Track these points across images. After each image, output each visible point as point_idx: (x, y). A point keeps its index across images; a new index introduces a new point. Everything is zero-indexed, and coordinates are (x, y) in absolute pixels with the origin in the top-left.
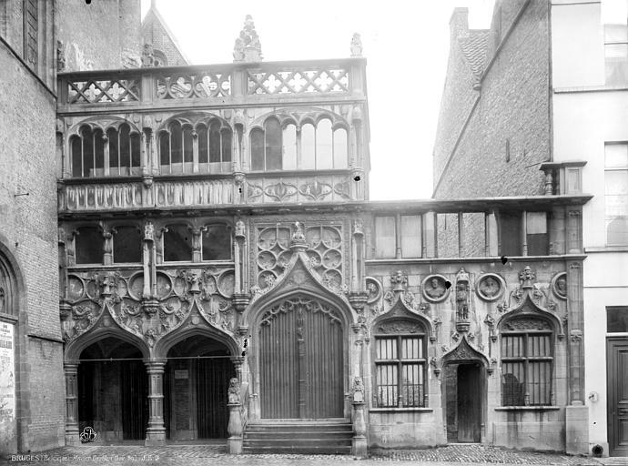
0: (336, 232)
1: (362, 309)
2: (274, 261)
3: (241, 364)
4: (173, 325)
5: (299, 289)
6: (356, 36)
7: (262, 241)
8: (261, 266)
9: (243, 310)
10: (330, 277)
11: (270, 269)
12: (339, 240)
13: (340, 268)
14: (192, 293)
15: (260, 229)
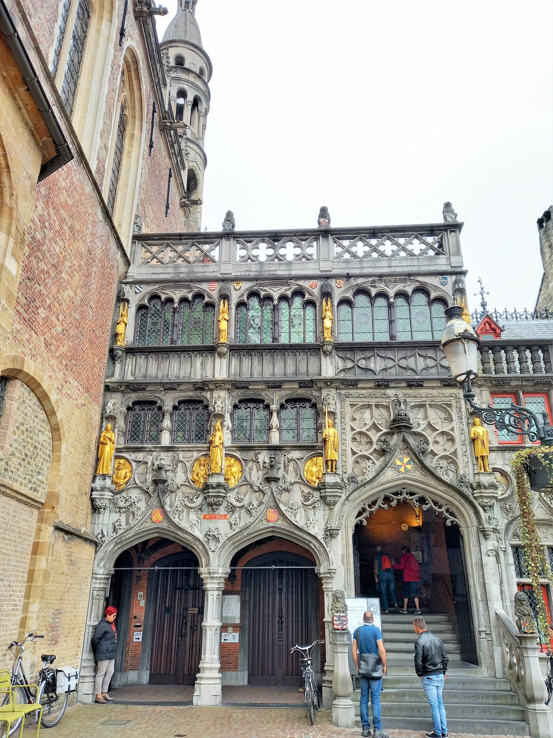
0: (446, 411)
1: (491, 507)
2: (371, 443)
3: (332, 578)
4: (243, 520)
5: (404, 478)
6: (447, 206)
7: (354, 419)
8: (355, 450)
9: (335, 503)
10: (444, 463)
11: (367, 453)
12: (450, 419)
13: (455, 453)
14: (268, 480)
15: (352, 405)
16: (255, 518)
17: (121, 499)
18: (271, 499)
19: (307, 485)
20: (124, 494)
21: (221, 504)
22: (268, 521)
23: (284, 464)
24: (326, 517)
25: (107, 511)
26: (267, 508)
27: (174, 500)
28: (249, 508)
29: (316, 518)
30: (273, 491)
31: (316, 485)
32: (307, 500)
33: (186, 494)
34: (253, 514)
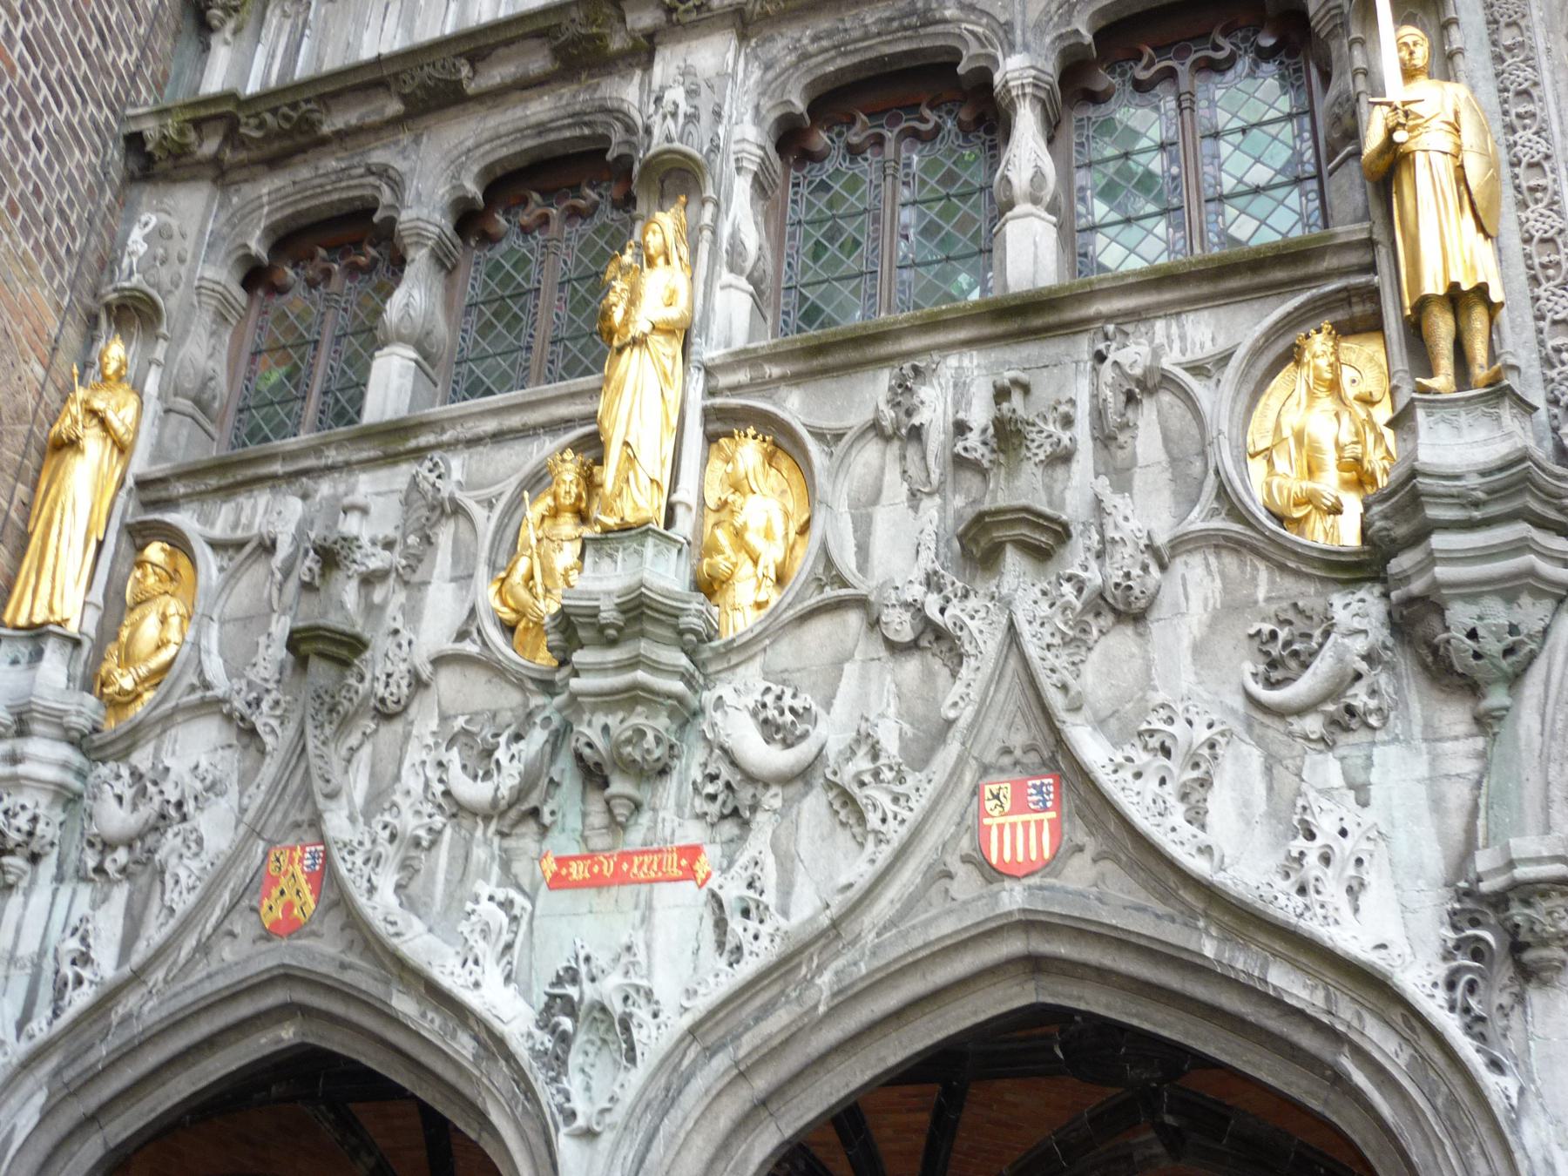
16: (885, 853)
17: (119, 787)
18: (1009, 696)
19: (1274, 540)
20: (142, 758)
21: (664, 772)
22: (993, 874)
23: (1099, 414)
24: (1458, 795)
25: (48, 867)
26: (985, 770)
27: (392, 769)
28: (846, 777)
29: (1369, 816)
30: (1021, 620)
31: (1347, 533)
32: (1277, 669)
33: (460, 722)
34: (873, 819)
